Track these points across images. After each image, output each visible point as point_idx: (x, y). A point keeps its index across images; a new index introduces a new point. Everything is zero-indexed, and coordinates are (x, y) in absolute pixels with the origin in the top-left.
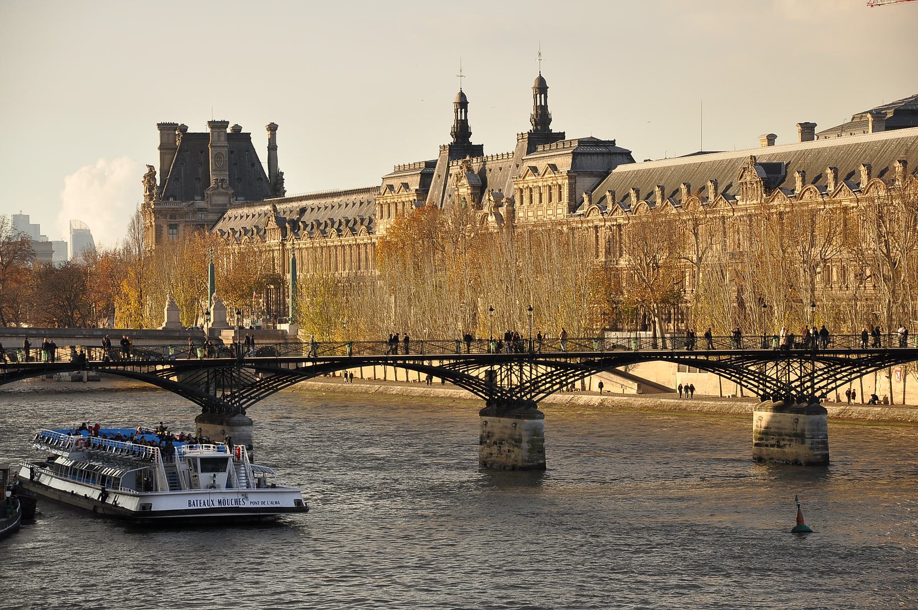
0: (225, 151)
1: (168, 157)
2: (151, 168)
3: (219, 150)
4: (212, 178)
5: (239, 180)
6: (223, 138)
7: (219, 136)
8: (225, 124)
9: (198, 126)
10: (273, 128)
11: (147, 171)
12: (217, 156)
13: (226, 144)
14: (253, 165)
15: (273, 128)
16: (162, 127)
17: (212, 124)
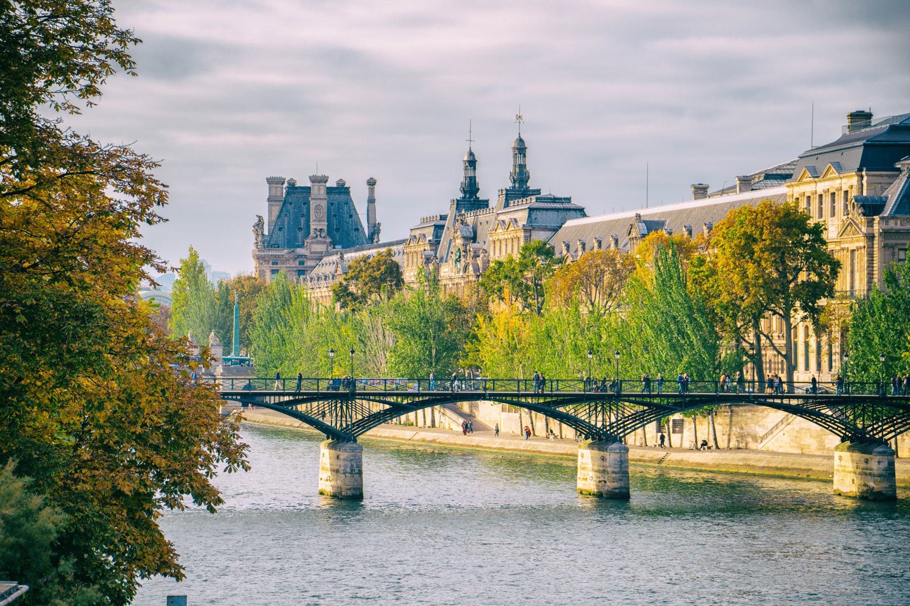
0: (324, 204)
1: (276, 210)
2: (260, 218)
3: (318, 202)
4: (312, 227)
5: (338, 230)
6: (323, 191)
7: (319, 189)
8: (325, 180)
9: (303, 182)
10: (372, 183)
11: (256, 220)
12: (318, 207)
13: (325, 196)
14: (351, 216)
15: (372, 183)
16: (273, 182)
17: (314, 179)
